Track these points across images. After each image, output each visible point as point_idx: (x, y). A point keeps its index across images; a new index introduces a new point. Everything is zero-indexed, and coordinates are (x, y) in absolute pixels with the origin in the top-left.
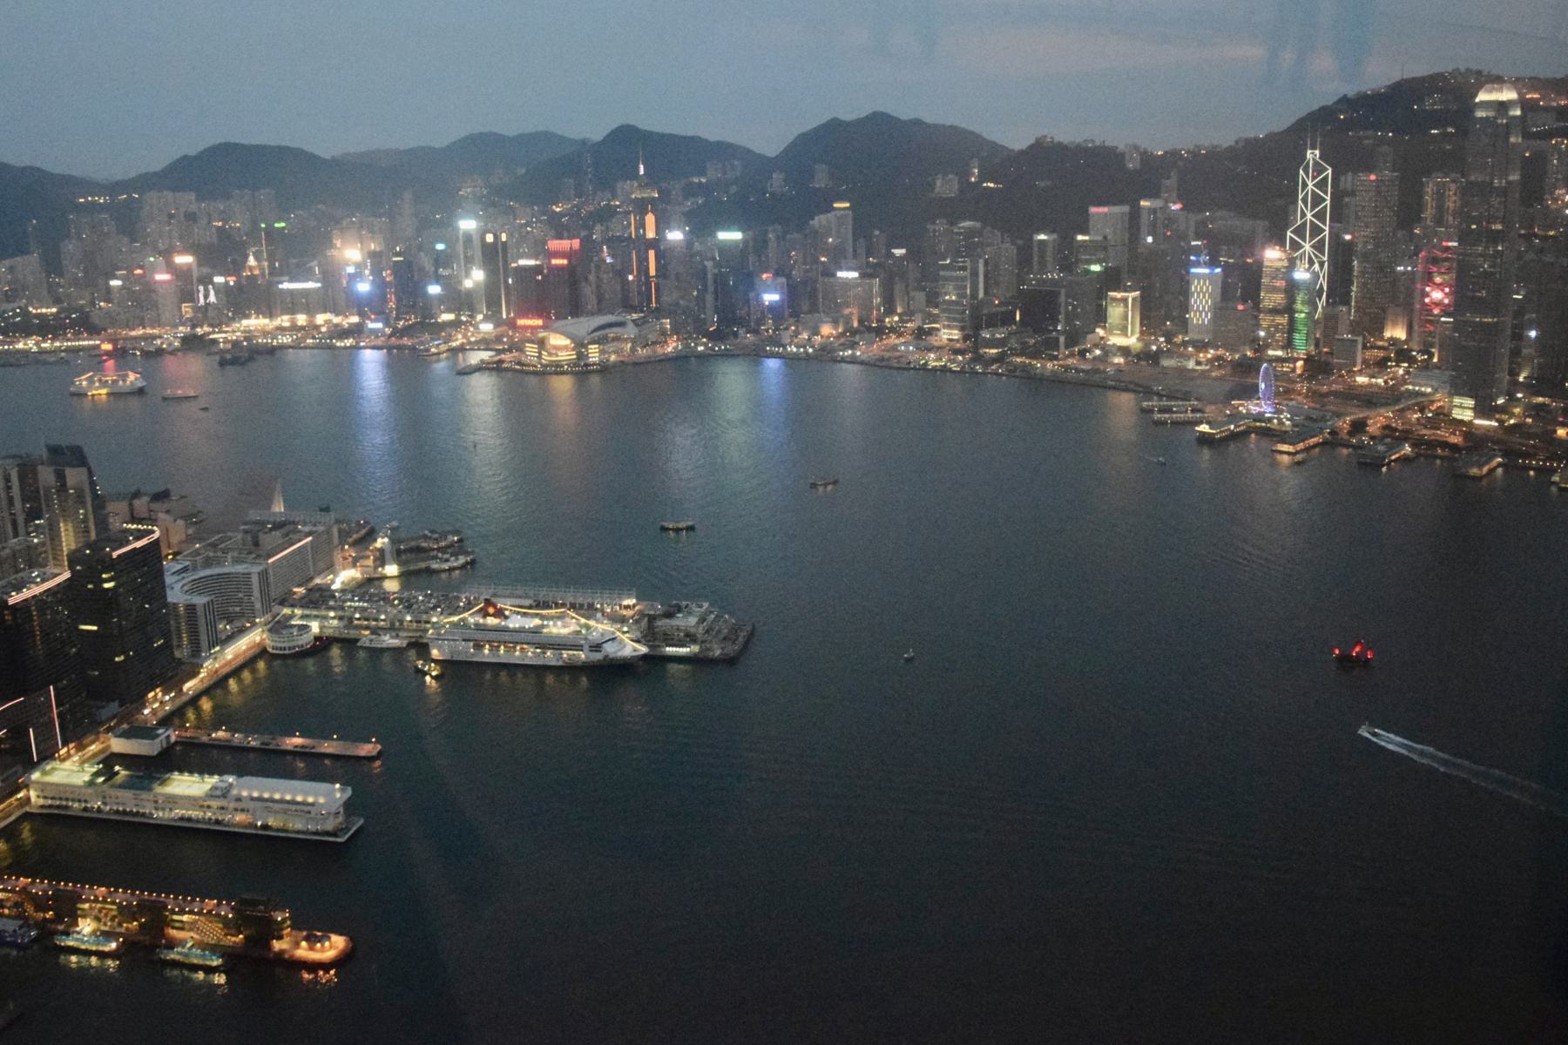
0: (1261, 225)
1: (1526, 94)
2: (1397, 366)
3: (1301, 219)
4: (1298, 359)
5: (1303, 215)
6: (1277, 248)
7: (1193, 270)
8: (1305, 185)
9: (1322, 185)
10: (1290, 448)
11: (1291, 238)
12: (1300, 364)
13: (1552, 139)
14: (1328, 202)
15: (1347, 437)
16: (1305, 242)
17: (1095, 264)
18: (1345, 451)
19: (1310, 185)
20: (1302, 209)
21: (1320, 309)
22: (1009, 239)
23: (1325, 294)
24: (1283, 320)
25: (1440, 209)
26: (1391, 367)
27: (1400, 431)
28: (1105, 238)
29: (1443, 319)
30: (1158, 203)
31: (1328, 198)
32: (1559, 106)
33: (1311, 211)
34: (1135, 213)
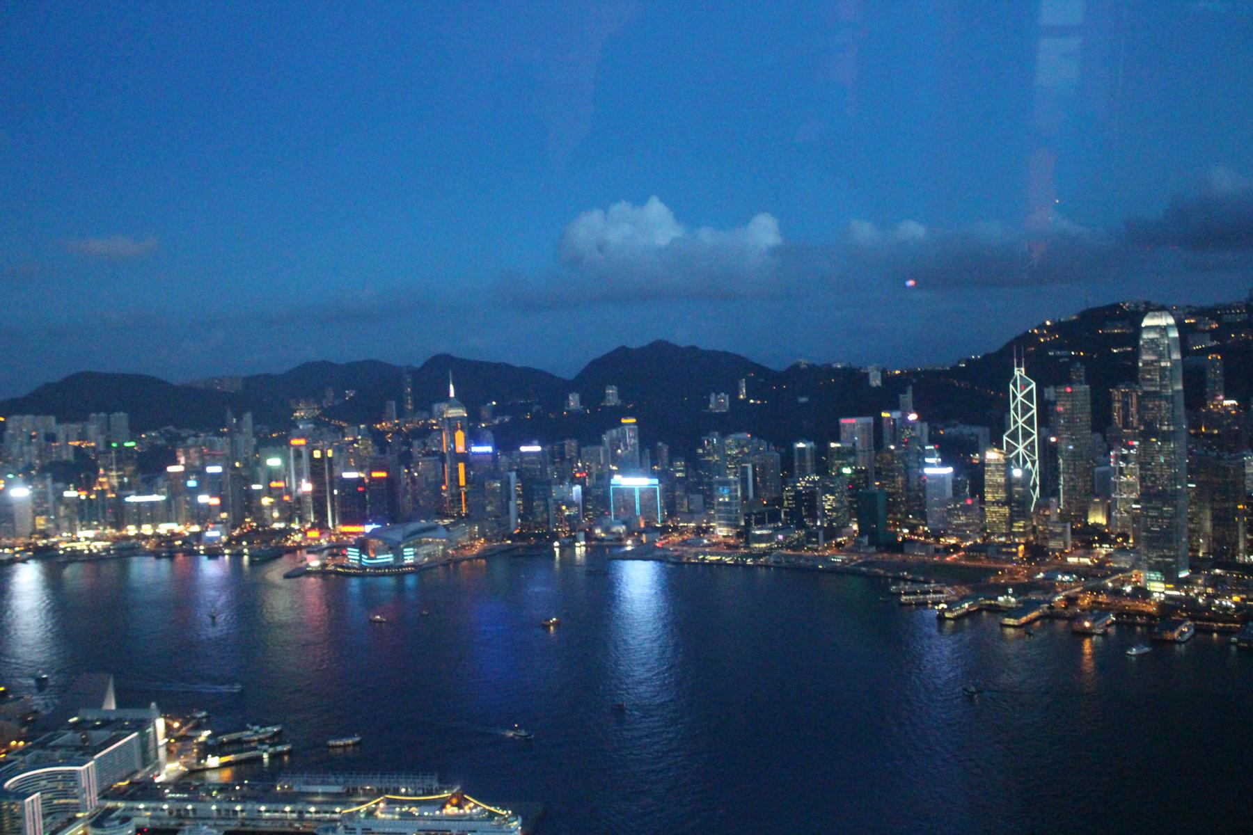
0: (981, 432)
3: (1014, 424)
4: (1019, 544)
5: (1016, 422)
6: (996, 450)
7: (928, 471)
8: (1015, 397)
9: (1028, 396)
11: (1007, 442)
12: (1021, 547)
14: (1035, 411)
16: (1018, 444)
17: (846, 467)
18: (1062, 624)
21: (1035, 500)
22: (774, 448)
23: (1038, 488)
25: (1126, 416)
27: (1105, 604)
28: (854, 445)
29: (1134, 506)
30: (897, 415)
31: (1034, 407)
32: (1211, 328)
33: (1022, 417)
34: (879, 421)
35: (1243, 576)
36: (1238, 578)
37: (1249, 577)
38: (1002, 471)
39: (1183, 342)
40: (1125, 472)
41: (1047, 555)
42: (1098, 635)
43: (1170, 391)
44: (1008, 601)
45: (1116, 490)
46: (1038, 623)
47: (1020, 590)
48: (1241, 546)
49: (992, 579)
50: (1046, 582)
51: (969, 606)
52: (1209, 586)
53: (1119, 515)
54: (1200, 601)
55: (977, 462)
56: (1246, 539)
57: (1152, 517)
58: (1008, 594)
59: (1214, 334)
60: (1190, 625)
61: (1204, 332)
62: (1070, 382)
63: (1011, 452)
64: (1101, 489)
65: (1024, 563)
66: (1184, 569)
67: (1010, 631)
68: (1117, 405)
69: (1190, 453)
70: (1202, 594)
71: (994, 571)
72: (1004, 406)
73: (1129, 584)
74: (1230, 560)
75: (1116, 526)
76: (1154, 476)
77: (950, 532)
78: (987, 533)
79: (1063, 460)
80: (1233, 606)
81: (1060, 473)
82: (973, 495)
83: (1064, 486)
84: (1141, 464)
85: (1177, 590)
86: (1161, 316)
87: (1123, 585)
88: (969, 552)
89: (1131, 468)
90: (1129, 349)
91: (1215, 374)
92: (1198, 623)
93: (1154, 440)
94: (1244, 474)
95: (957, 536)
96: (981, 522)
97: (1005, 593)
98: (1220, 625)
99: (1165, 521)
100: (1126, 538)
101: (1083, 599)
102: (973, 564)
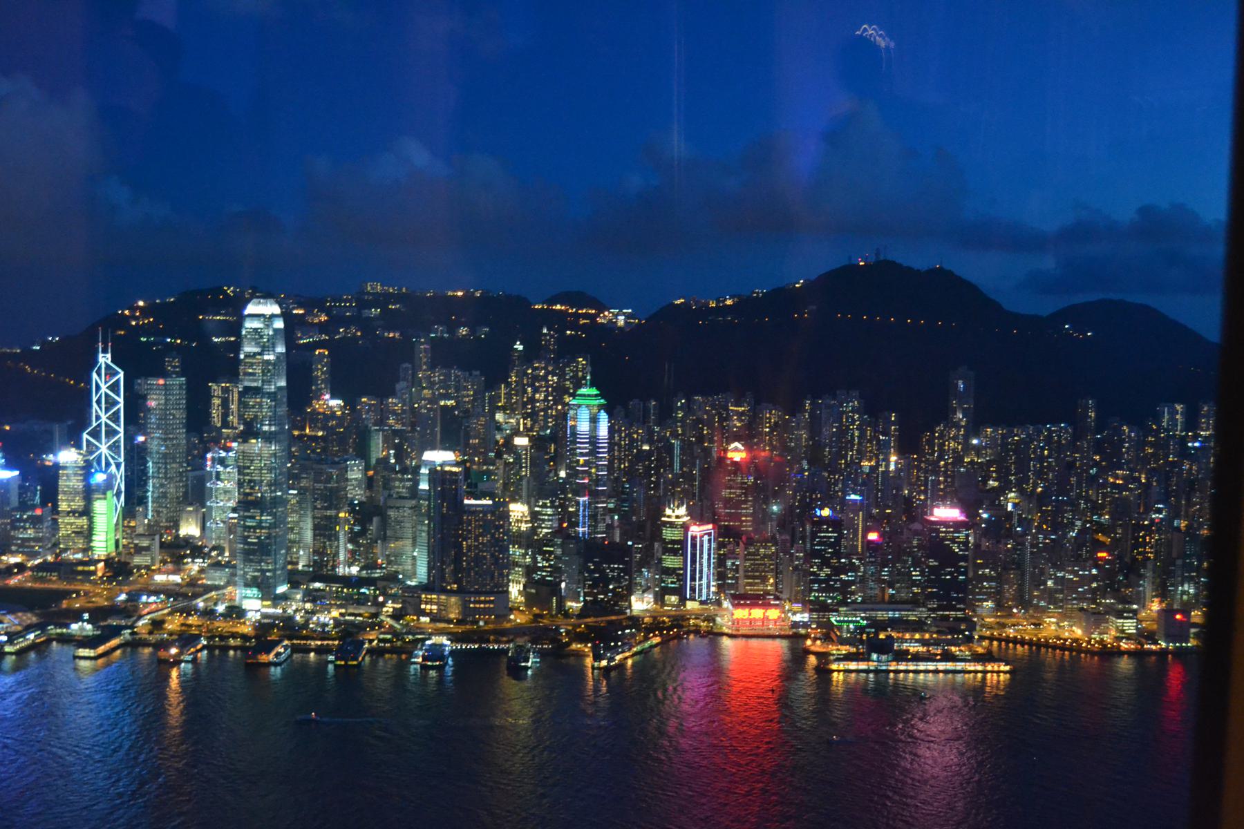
1: (294, 308)
2: (193, 562)
4: (99, 561)
5: (98, 418)
9: (114, 388)
10: (91, 653)
11: (87, 441)
12: (101, 565)
13: (315, 351)
14: (121, 405)
15: (147, 636)
16: (101, 444)
18: (147, 651)
19: (104, 388)
20: (96, 411)
24: (83, 521)
25: (225, 415)
26: (187, 563)
29: (232, 515)
31: (121, 400)
35: (343, 588)
36: (337, 592)
37: (348, 590)
38: (81, 475)
39: (288, 335)
40: (222, 477)
41: (131, 573)
42: (187, 662)
43: (273, 387)
44: (82, 629)
45: (211, 497)
46: (118, 652)
47: (98, 615)
48: (342, 558)
49: (65, 604)
50: (129, 604)
51: (35, 636)
52: (308, 601)
53: (214, 526)
54: (298, 618)
55: (51, 464)
56: (346, 548)
57: (250, 527)
58: (84, 621)
59: (322, 327)
60: (287, 645)
61: (313, 325)
62: (164, 374)
63: (91, 453)
64: (196, 494)
65: (103, 583)
66: (282, 583)
67: (83, 664)
68: (216, 401)
69: (290, 456)
70: (301, 610)
71: (66, 594)
72: (83, 399)
73: (222, 603)
74: (330, 573)
75: (212, 539)
76: (254, 481)
77: (14, 548)
78: (60, 548)
79: (153, 463)
80: (332, 622)
81: (148, 478)
82: (43, 504)
83: (153, 492)
84: (239, 467)
85: (275, 606)
86: (266, 304)
87: (216, 604)
88: (37, 572)
89: (229, 472)
90: (232, 339)
91: (321, 371)
92: (295, 642)
93: (254, 441)
94: (347, 480)
95: (23, 553)
96: (54, 535)
97: (81, 619)
98: (319, 643)
99: (263, 531)
100: (221, 553)
101: (172, 622)
102: (42, 586)
